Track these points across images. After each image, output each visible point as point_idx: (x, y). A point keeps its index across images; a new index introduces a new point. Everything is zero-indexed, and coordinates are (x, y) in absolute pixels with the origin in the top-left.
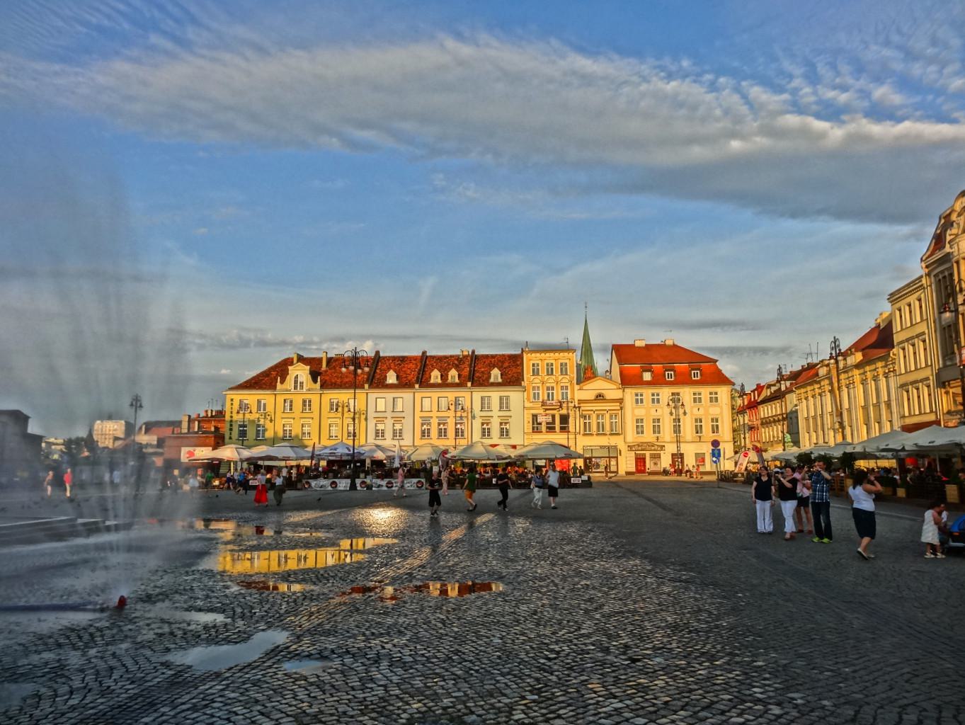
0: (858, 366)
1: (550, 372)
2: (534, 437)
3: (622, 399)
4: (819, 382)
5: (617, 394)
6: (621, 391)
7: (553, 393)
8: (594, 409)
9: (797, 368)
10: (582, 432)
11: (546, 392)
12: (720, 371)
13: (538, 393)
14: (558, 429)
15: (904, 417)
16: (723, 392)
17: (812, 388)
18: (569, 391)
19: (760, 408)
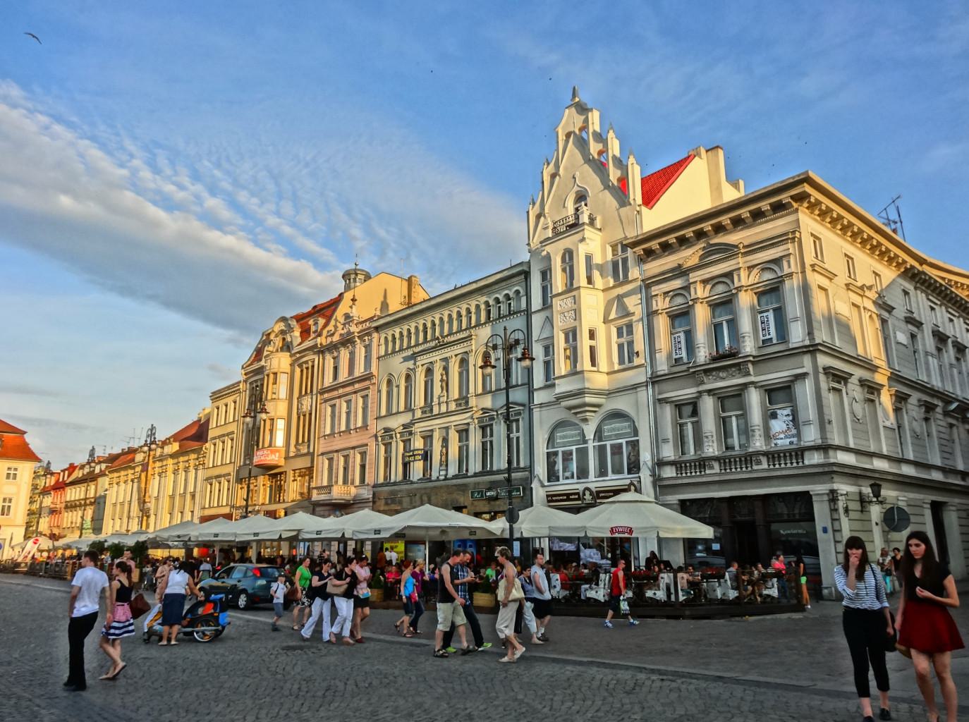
0: (173, 456)
4: (134, 468)
9: (117, 451)
12: (26, 445)
15: (204, 508)
16: (26, 469)
17: (125, 473)
19: (68, 490)
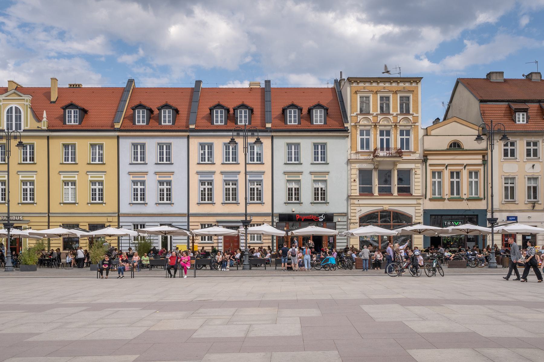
1: (384, 110)
2: (361, 202)
7: (388, 140)
8: (447, 162)
10: (429, 196)
11: (379, 138)
13: (368, 140)
18: (412, 137)
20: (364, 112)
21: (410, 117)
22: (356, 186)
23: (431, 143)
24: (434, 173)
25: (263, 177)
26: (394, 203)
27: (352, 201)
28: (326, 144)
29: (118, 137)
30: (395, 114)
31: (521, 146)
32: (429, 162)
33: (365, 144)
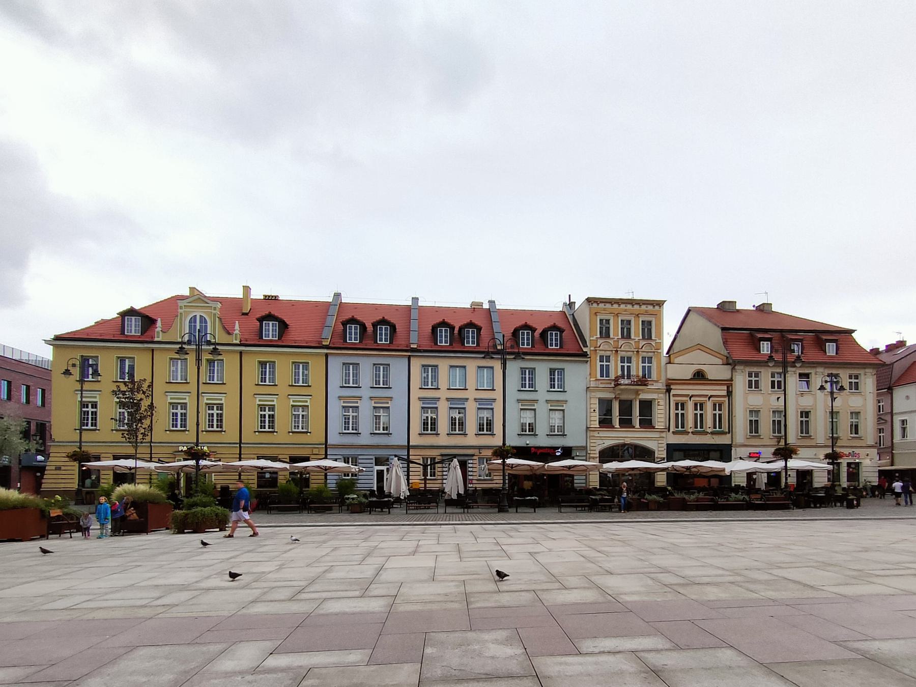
2: (601, 434)
3: (731, 380)
5: (723, 372)
6: (729, 367)
7: (629, 367)
8: (691, 393)
13: (608, 366)
14: (636, 422)
18: (654, 365)
20: (605, 333)
21: (653, 343)
22: (596, 417)
23: (674, 372)
24: (677, 404)
25: (494, 405)
26: (635, 436)
27: (592, 434)
28: (563, 369)
29: (327, 355)
30: (637, 339)
31: (766, 378)
32: (673, 392)
33: (605, 371)
